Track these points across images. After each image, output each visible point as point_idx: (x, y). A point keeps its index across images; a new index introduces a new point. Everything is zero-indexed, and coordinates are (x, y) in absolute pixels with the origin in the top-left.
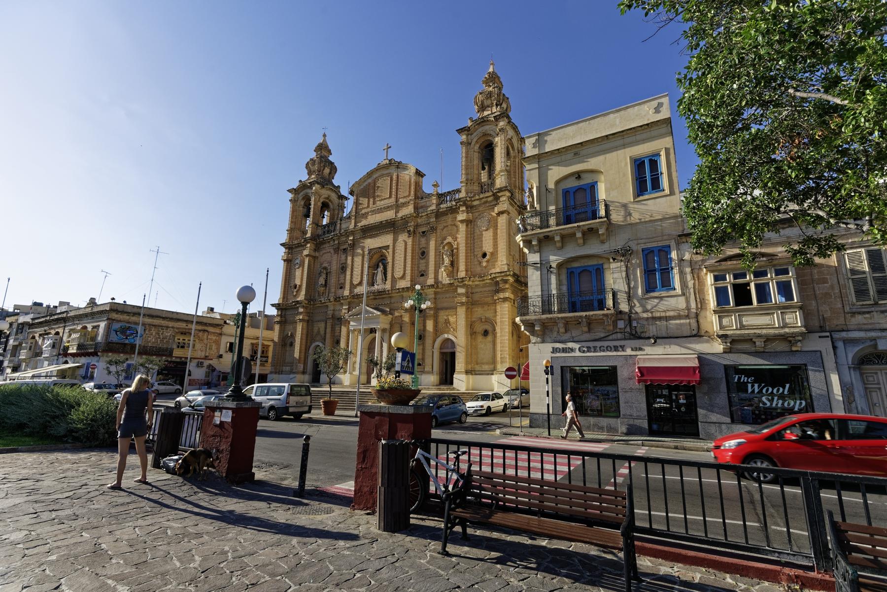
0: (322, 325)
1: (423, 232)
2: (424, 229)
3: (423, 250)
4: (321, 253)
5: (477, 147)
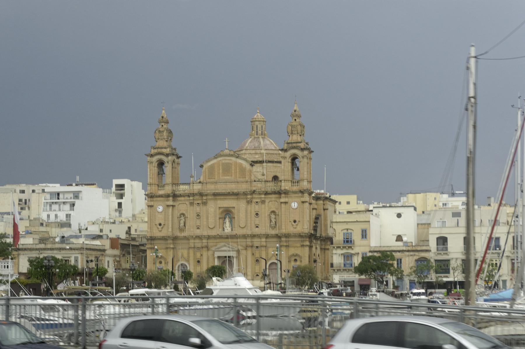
0: (185, 252)
1: (257, 202)
2: (257, 200)
3: (257, 212)
4: (178, 203)
5: (290, 160)
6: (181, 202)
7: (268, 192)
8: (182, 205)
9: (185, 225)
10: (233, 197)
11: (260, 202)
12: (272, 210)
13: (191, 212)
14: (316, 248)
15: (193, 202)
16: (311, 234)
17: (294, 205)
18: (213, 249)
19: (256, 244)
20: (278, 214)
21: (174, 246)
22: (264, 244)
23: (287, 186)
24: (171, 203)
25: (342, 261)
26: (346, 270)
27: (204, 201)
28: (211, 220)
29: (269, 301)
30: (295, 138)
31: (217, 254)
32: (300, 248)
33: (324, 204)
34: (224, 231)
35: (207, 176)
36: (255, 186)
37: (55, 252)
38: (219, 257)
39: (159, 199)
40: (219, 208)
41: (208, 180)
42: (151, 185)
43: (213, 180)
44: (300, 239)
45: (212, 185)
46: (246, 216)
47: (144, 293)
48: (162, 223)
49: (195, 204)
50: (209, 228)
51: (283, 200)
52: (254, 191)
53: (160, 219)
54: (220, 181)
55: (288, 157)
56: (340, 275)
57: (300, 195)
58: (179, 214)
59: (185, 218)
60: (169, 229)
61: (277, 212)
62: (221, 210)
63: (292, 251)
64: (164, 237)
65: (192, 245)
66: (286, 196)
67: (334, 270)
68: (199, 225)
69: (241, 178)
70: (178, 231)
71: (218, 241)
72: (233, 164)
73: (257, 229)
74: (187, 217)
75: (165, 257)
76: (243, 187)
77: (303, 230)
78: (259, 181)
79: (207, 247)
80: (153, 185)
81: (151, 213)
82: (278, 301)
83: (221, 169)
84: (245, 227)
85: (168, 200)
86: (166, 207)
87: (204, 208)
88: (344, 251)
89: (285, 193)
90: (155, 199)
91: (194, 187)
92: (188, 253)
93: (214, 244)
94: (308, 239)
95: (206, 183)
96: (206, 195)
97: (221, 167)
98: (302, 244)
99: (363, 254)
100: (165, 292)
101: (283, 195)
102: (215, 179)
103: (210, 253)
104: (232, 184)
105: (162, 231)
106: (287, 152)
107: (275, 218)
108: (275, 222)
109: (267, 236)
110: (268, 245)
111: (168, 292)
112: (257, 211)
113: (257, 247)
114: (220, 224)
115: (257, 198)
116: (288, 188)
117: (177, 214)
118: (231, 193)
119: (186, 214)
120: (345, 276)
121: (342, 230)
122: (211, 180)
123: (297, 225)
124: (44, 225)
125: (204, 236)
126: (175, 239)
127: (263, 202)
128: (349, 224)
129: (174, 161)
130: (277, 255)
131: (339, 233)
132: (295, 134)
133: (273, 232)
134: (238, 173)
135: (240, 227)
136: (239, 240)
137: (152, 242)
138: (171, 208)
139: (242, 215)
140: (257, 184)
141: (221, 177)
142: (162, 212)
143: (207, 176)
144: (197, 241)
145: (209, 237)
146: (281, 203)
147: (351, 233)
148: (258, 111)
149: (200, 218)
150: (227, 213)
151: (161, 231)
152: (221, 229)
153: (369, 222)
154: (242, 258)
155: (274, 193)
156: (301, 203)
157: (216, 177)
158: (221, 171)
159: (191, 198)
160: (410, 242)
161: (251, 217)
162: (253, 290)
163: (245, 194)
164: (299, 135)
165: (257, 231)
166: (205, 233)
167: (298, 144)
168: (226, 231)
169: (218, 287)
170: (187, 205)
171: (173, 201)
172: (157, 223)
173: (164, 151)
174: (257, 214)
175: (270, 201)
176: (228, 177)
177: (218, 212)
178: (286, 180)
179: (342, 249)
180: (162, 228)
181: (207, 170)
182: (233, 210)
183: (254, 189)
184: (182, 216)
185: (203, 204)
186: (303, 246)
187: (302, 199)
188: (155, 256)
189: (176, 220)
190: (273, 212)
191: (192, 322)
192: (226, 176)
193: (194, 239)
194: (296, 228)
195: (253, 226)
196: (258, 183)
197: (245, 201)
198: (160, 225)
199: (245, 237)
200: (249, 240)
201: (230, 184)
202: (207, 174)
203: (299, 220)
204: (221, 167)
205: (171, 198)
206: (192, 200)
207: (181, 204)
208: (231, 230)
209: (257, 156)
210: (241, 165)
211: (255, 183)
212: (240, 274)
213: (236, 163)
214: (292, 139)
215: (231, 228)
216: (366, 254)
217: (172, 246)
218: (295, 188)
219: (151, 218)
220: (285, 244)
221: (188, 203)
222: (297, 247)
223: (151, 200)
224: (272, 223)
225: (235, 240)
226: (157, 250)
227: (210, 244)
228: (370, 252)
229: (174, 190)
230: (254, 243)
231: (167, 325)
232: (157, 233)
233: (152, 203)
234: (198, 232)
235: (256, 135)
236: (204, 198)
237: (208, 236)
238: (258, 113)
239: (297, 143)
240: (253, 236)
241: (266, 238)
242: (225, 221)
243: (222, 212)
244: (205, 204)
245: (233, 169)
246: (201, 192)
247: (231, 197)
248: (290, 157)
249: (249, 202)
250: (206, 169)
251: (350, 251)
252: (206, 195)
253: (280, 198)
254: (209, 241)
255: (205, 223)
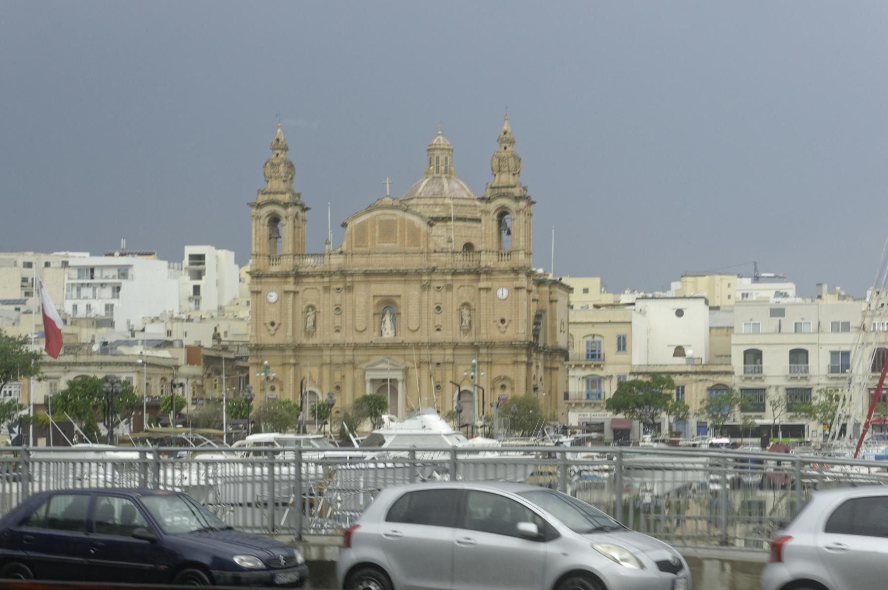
0: (315, 371)
1: (439, 288)
2: (439, 285)
3: (437, 305)
4: (305, 287)
5: (495, 217)
6: (308, 287)
8: (311, 291)
9: (314, 325)
10: (397, 278)
11: (443, 287)
12: (464, 301)
13: (326, 303)
14: (537, 367)
15: (330, 287)
16: (530, 342)
17: (503, 293)
18: (364, 366)
19: (438, 359)
20: (473, 308)
21: (296, 360)
22: (450, 359)
23: (491, 261)
24: (291, 287)
25: (584, 390)
26: (590, 404)
27: (348, 284)
28: (360, 317)
29: (481, 456)
30: (505, 179)
31: (370, 375)
32: (511, 367)
33: (551, 293)
34: (381, 334)
35: (354, 242)
36: (435, 261)
37: (93, 368)
38: (373, 381)
39: (270, 280)
40: (374, 296)
41: (355, 249)
42: (258, 257)
43: (364, 249)
44: (512, 351)
45: (362, 258)
46: (420, 312)
47: (272, 440)
48: (277, 322)
49: (333, 289)
50: (357, 330)
51: (482, 284)
52: (434, 269)
53: (272, 314)
54: (377, 251)
55: (492, 213)
56: (581, 413)
57: (512, 276)
58: (304, 307)
59: (315, 313)
60: (287, 332)
61: (473, 304)
62: (377, 300)
63: (498, 371)
64: (280, 345)
65: (327, 359)
66: (488, 277)
67: (571, 404)
68: (340, 325)
69: (411, 246)
70: (303, 335)
71: (371, 352)
72: (398, 221)
73: (438, 333)
74: (319, 312)
75: (281, 379)
76: (415, 262)
77: (516, 337)
78: (442, 252)
79: (353, 364)
80: (261, 257)
81: (257, 304)
82: (495, 455)
83: (377, 231)
84: (417, 330)
85: (286, 283)
86: (283, 294)
87: (349, 296)
88: (588, 372)
89: (486, 273)
90: (264, 280)
91: (331, 260)
92: (321, 374)
93: (365, 358)
94: (524, 352)
95: (352, 255)
96: (352, 275)
97: (377, 227)
98: (514, 359)
99: (619, 378)
100: (309, 439)
101: (483, 277)
102: (367, 246)
103: (358, 373)
104: (397, 257)
105: (277, 335)
106: (490, 202)
107: (470, 315)
108: (470, 322)
109: (455, 346)
110: (457, 361)
111: (314, 439)
112: (439, 303)
113: (438, 364)
114: (374, 325)
115: (439, 280)
116: (492, 263)
117: (301, 306)
118: (395, 271)
119: (317, 307)
120: (589, 414)
121: (584, 337)
122: (361, 249)
123: (506, 327)
124: (69, 322)
125: (348, 344)
126: (298, 348)
127: (449, 287)
128: (596, 326)
129: (296, 216)
130: (472, 377)
131: (580, 342)
132: (504, 172)
133: (466, 339)
134: (406, 238)
135: (409, 329)
136: (407, 352)
137: (259, 354)
138: (291, 295)
139: (413, 309)
140: (440, 256)
141: (377, 244)
142: (275, 303)
143: (354, 242)
144: (335, 352)
145: (356, 347)
146: (480, 289)
147: (600, 342)
148: (440, 132)
149: (341, 313)
150: (388, 305)
151: (274, 334)
152: (376, 334)
153: (630, 323)
154: (414, 381)
155: (469, 272)
156: (514, 290)
157: (369, 244)
158: (377, 234)
159: (326, 279)
160: (699, 358)
161: (428, 313)
162: (454, 436)
163: (418, 273)
164: (511, 174)
165: (438, 337)
166: (350, 339)
167: (510, 190)
168: (385, 336)
169: (393, 432)
170: (319, 291)
171: (296, 283)
172: (268, 321)
173: (280, 197)
174: (438, 308)
175: (460, 287)
176: (390, 245)
177: (372, 303)
178: (488, 250)
179: (584, 369)
180: (276, 330)
181: (353, 231)
182: (397, 301)
183: (434, 264)
184: (310, 309)
185: (346, 289)
186: (516, 363)
187: (515, 282)
188: (264, 378)
189: (300, 317)
190: (466, 304)
191: (518, 493)
192: (386, 243)
193: (331, 349)
194: (504, 332)
196: (441, 254)
197: (418, 286)
198: (273, 324)
199: (418, 346)
200: (424, 352)
201: (393, 255)
202: (353, 238)
203: (510, 319)
204: (377, 227)
205: (291, 280)
206: (327, 282)
207: (309, 289)
208: (394, 335)
209: (437, 209)
210: (411, 223)
211: (435, 255)
212: (431, 409)
213: (403, 221)
214: (499, 181)
215: (393, 331)
216: (624, 377)
217: (292, 361)
218: (504, 265)
219: (256, 312)
220: (486, 359)
221: (320, 287)
222: (507, 365)
223: (257, 283)
224: (463, 324)
225: (401, 352)
226: (268, 367)
227: (358, 359)
228: (632, 373)
229: (296, 266)
230: (433, 357)
231: (471, 498)
232: (267, 339)
233: (258, 288)
234: (337, 338)
235: (436, 173)
236: (349, 279)
237: (355, 344)
238: (439, 135)
239: (508, 187)
240: (433, 345)
241: (454, 349)
242: (384, 320)
243: (379, 304)
244: (349, 289)
245: (398, 229)
246: (343, 269)
247: (394, 279)
248: (496, 211)
249: (425, 287)
250: (352, 229)
251: (598, 372)
252: (352, 275)
253: (479, 280)
254: (356, 353)
255: (349, 322)
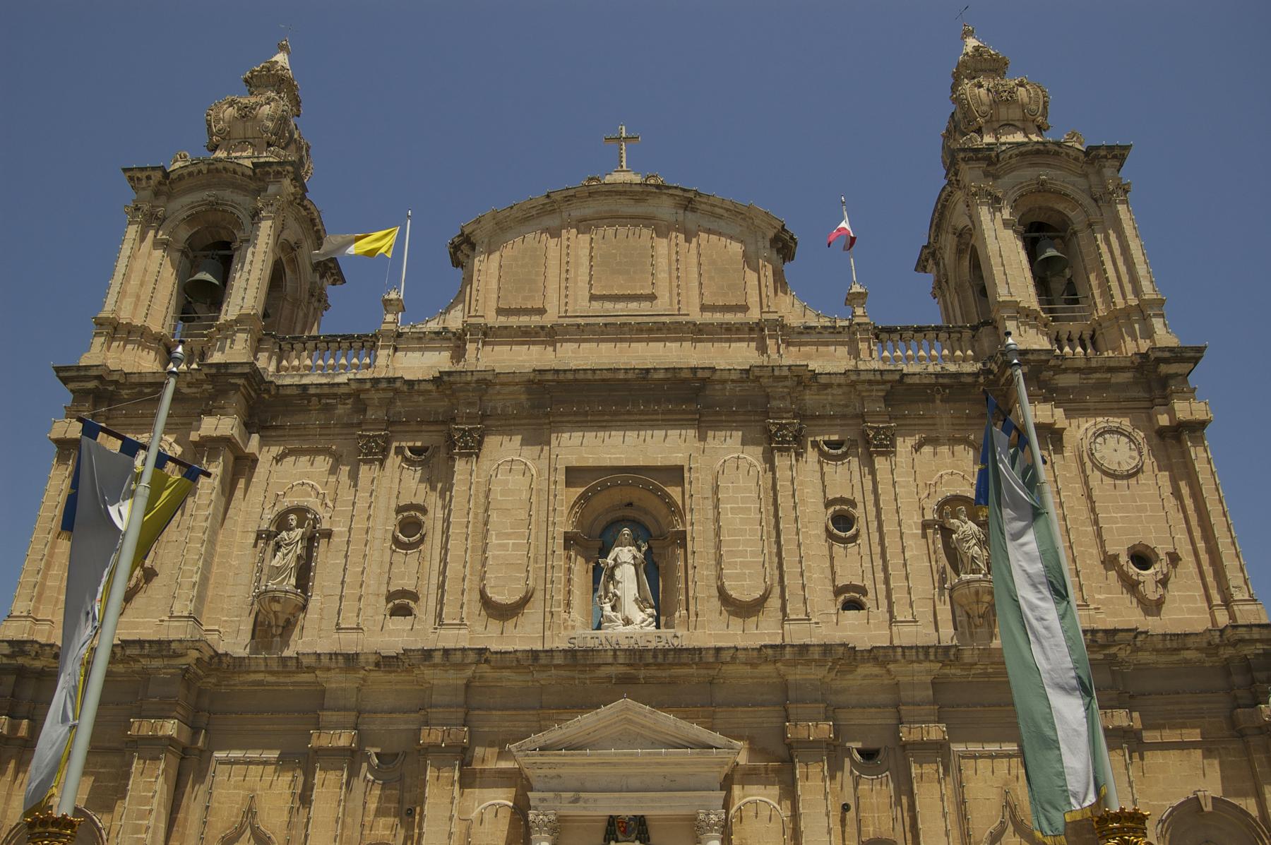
7: (908, 380)
68: (409, 585)
123: (1164, 582)
149: (421, 541)
171: (249, 426)
195: (822, 598)
